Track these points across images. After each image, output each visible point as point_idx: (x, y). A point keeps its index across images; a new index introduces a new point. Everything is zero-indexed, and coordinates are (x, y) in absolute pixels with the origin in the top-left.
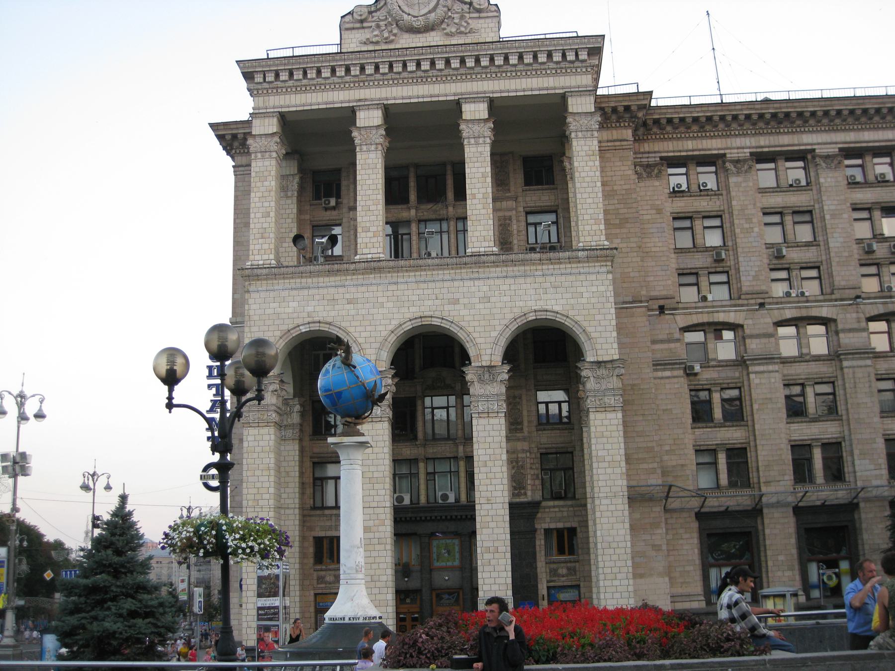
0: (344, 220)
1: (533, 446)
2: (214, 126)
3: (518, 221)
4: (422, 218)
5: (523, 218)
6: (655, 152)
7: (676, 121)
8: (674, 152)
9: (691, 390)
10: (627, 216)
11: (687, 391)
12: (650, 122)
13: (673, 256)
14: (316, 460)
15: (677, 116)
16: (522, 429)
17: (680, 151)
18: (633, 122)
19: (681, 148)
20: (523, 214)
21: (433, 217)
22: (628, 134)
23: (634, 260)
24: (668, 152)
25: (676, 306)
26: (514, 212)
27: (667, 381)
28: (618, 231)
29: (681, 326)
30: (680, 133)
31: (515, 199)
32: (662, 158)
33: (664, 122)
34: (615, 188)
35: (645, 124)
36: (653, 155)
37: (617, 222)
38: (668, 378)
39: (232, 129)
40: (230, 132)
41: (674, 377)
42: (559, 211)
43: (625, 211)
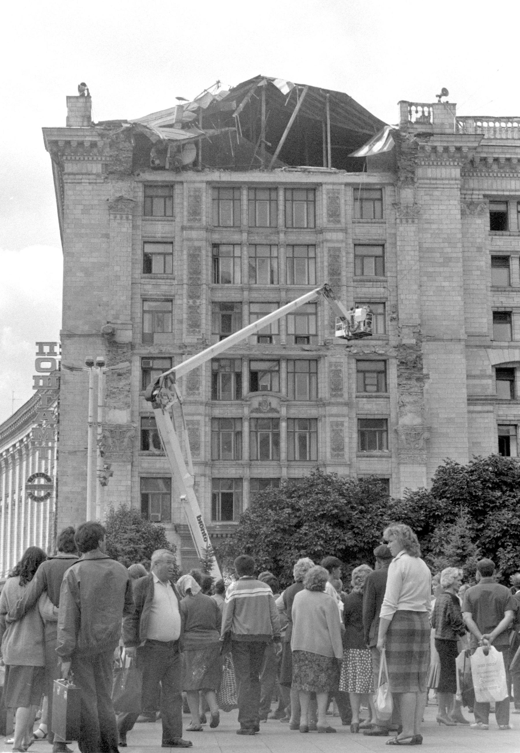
0: (176, 239)
1: (352, 471)
2: (44, 130)
3: (348, 253)
4: (253, 242)
5: (351, 250)
6: (479, 190)
7: (503, 161)
8: (497, 190)
9: (499, 425)
10: (450, 255)
11: (496, 426)
12: (477, 160)
13: (490, 293)
14: (144, 475)
15: (504, 156)
16: (343, 455)
17: (503, 191)
18: (462, 162)
19: (504, 188)
20: (352, 246)
21: (264, 242)
22: (456, 172)
23: (455, 298)
24: (491, 190)
25: (490, 343)
26: (344, 245)
27: (478, 415)
28: (441, 269)
29: (493, 364)
30: (505, 172)
31: (345, 230)
32: (485, 196)
33: (490, 161)
34: (441, 227)
35: (472, 162)
36: (477, 192)
37: (441, 260)
38: (480, 412)
39: (65, 136)
40: (64, 139)
41: (484, 412)
42: (387, 245)
43: (449, 250)
